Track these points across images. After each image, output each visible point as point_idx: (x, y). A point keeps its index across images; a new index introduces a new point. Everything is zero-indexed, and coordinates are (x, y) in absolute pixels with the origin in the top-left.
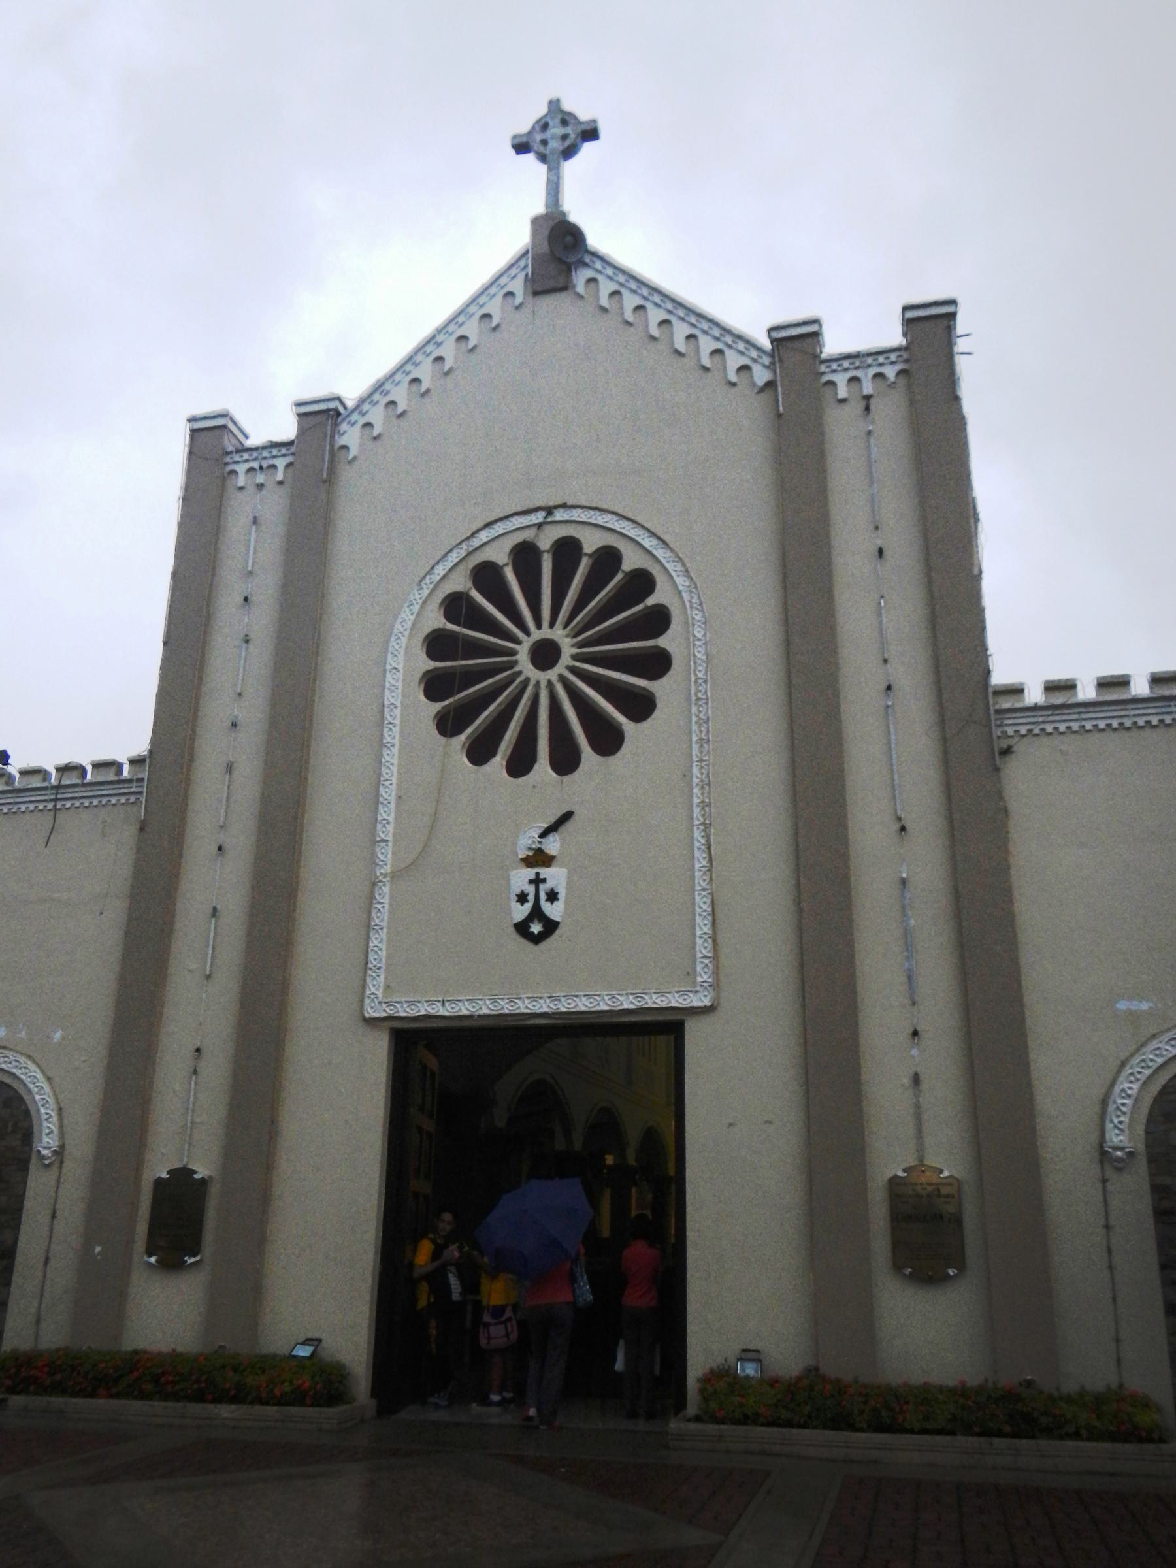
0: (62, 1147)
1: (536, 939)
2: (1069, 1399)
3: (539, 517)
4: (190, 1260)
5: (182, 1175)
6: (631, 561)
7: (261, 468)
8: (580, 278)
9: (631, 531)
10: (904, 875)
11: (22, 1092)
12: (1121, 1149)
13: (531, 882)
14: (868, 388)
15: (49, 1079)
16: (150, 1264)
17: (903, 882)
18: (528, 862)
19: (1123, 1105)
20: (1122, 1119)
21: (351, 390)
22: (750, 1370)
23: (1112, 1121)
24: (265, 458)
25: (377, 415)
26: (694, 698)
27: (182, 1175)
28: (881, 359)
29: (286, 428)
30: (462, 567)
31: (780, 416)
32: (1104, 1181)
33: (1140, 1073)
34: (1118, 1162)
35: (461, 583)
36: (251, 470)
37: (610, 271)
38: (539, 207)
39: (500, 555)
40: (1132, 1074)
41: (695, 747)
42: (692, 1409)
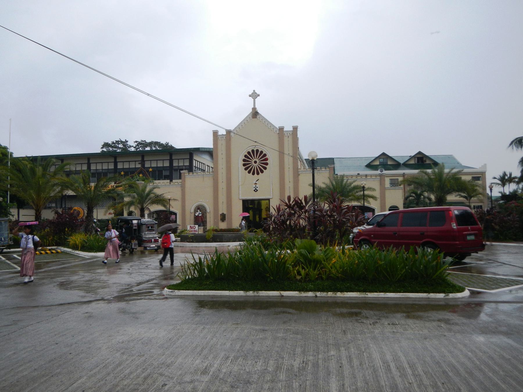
1: (256, 192)
3: (254, 147)
6: (264, 153)
8: (258, 116)
9: (265, 150)
18: (255, 184)
21: (232, 128)
35: (246, 154)
38: (253, 107)
39: (250, 151)
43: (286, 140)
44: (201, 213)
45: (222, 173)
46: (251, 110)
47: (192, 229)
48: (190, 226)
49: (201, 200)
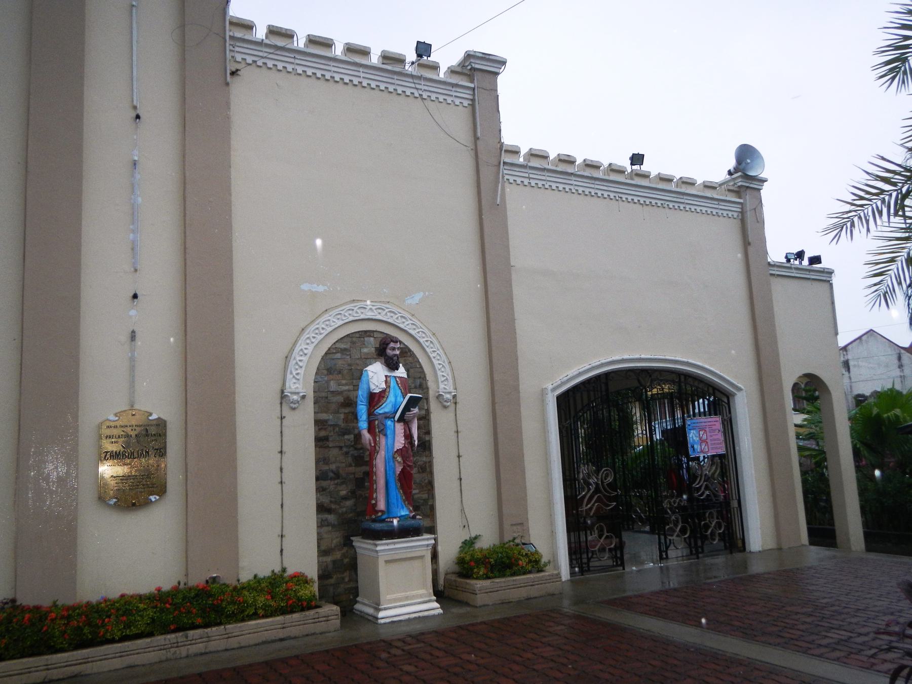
2: (248, 587)
10: (136, 158)
12: (298, 393)
17: (135, 163)
19: (300, 361)
20: (299, 371)
23: (291, 373)
32: (282, 418)
33: (314, 337)
34: (295, 404)
40: (308, 338)
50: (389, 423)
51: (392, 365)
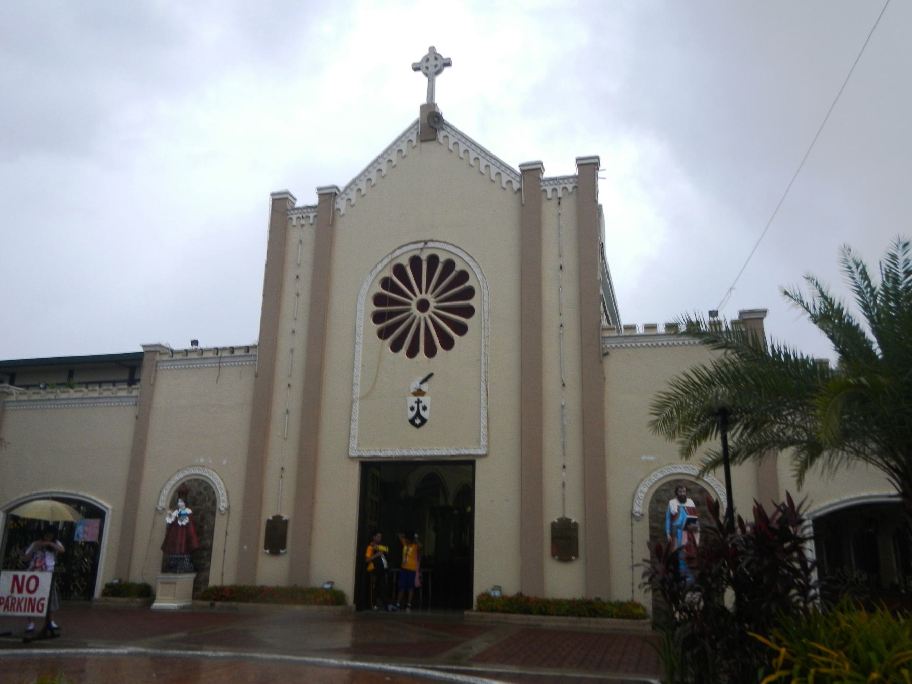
0: (229, 506)
1: (418, 426)
3: (421, 245)
4: (282, 551)
5: (277, 518)
6: (459, 266)
7: (303, 217)
8: (441, 135)
10: (563, 404)
11: (212, 485)
12: (639, 513)
13: (416, 402)
14: (560, 194)
15: (222, 479)
16: (266, 553)
17: (563, 407)
18: (415, 394)
21: (342, 183)
22: (497, 593)
24: (304, 213)
25: (353, 195)
26: (483, 327)
27: (277, 518)
28: (566, 181)
29: (314, 200)
30: (389, 266)
31: (523, 205)
32: (632, 525)
35: (389, 273)
36: (299, 218)
37: (453, 133)
38: (424, 101)
39: (405, 261)
41: (483, 348)
42: (475, 608)
43: (549, 210)
44: (189, 511)
45: (292, 351)
46: (415, 115)
47: (20, 591)
48: (15, 578)
49: (202, 460)
50: (679, 531)
51: (682, 500)
